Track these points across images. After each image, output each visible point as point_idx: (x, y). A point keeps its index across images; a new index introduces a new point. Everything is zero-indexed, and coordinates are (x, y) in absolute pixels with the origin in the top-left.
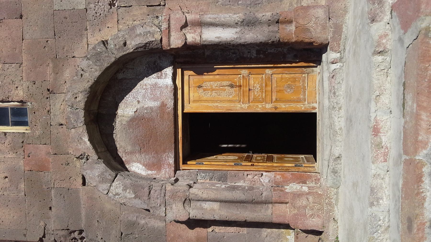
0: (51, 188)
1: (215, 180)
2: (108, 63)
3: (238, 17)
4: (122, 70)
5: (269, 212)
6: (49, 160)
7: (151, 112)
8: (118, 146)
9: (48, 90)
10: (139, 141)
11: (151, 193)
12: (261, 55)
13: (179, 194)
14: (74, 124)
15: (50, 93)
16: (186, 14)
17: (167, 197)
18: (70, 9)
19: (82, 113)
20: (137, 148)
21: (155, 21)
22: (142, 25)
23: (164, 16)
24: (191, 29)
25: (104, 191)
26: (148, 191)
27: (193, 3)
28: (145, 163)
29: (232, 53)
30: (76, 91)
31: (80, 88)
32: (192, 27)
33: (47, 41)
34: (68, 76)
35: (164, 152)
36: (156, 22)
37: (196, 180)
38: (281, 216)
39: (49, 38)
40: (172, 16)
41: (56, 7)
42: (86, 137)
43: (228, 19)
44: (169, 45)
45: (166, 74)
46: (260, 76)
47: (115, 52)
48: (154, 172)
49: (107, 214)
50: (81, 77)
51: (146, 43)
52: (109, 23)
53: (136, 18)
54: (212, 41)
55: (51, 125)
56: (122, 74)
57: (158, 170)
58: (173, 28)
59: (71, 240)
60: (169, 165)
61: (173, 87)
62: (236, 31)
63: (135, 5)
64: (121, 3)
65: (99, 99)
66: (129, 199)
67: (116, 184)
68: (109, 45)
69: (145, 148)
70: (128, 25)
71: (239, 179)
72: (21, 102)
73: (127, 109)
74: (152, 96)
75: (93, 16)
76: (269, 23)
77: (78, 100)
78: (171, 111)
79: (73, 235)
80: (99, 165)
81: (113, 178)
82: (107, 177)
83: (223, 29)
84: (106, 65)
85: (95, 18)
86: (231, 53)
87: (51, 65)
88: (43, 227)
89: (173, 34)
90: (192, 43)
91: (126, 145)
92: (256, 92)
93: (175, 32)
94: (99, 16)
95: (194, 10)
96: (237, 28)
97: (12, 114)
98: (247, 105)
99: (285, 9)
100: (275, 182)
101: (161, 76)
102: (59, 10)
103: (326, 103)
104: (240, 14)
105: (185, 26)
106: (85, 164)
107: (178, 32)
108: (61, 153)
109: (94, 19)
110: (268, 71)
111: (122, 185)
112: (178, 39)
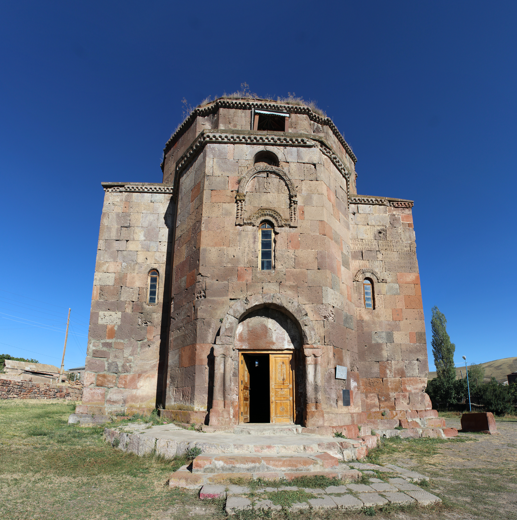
3: (319, 383)
5: (219, 399)
8: (251, 319)
9: (281, 282)
13: (228, 352)
17: (226, 345)
20: (251, 329)
35: (249, 344)
36: (317, 341)
40: (320, 350)
44: (305, 348)
46: (289, 394)
47: (302, 320)
60: (242, 346)
71: (235, 383)
72: (274, 267)
76: (316, 398)
79: (202, 292)
84: (295, 315)
87: (294, 284)
88: (207, 275)
89: (311, 350)
92: (280, 392)
97: (267, 261)
98: (273, 387)
103: (276, 427)
105: (315, 356)
110: (291, 398)
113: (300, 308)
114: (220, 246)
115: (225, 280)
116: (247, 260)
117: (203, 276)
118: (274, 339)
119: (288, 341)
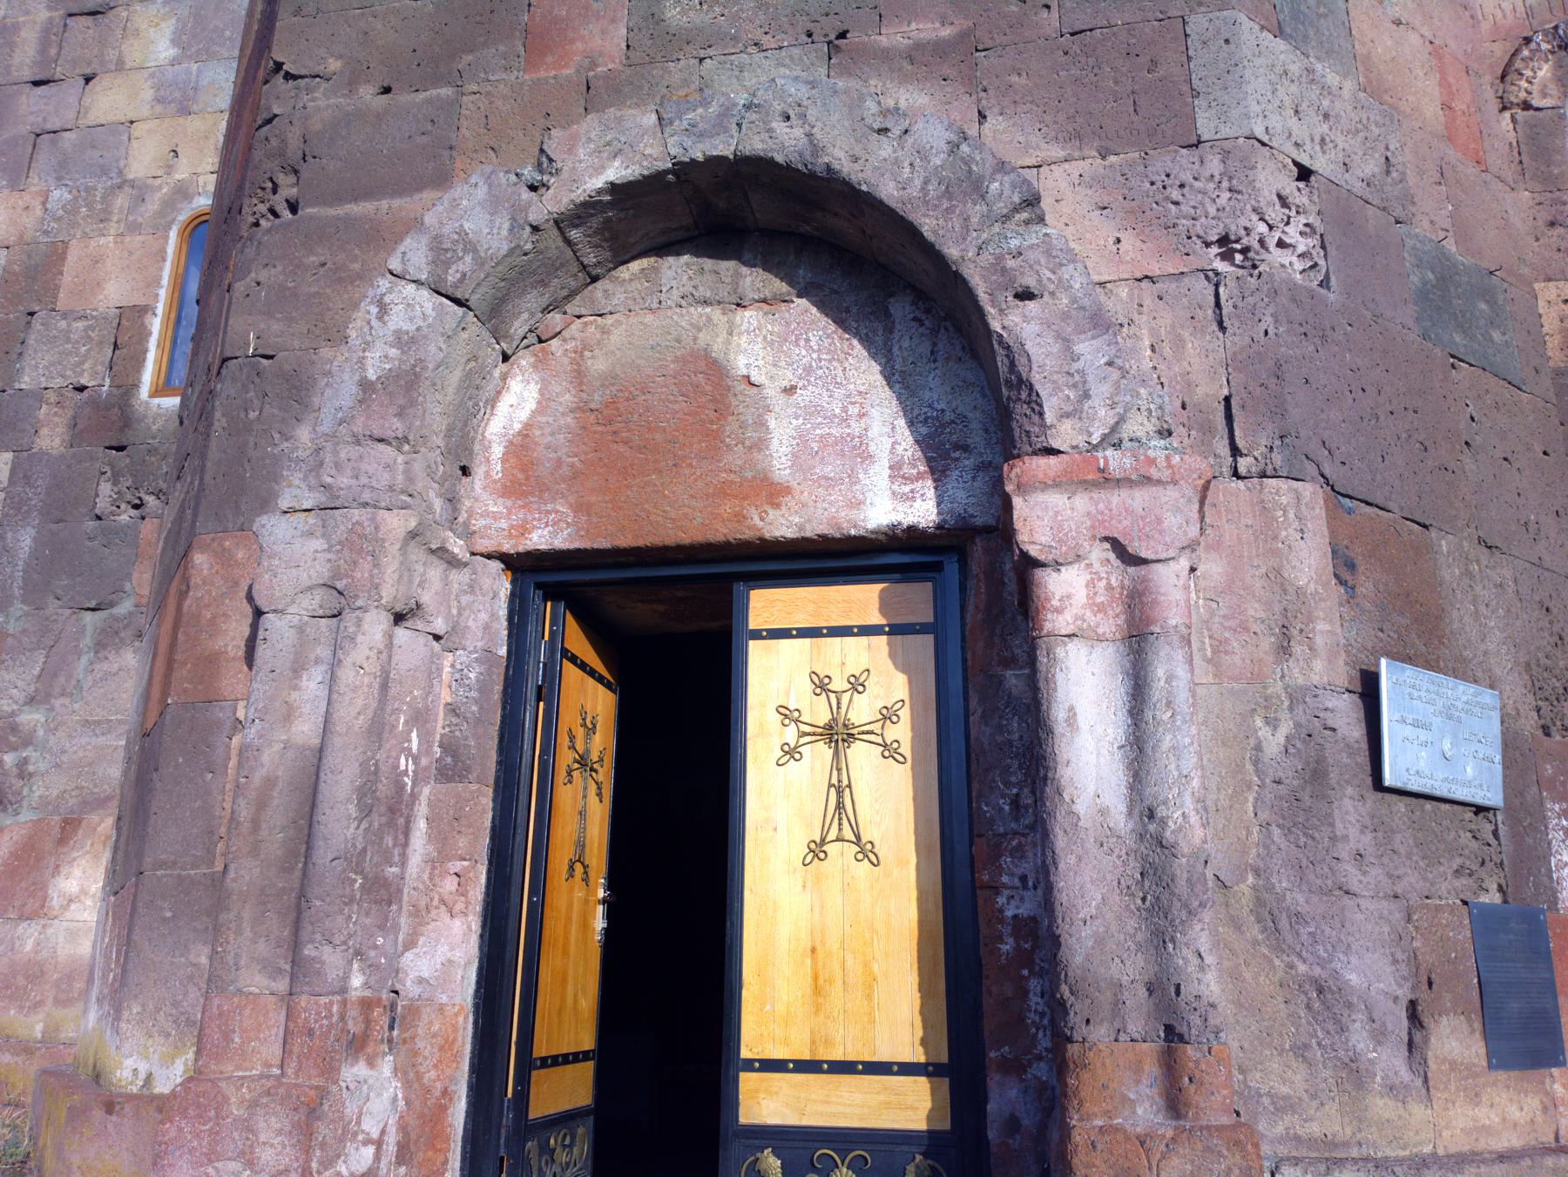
0: (459, 83)
1: (447, 729)
2: (935, 232)
4: (928, 311)
6: (566, 66)
7: (747, 443)
9: (842, 35)
10: (628, 400)
11: (381, 446)
12: (1011, 941)
14: (677, 123)
15: (829, 43)
16: (1184, 563)
18: (1193, 77)
19: (721, 147)
20: (597, 399)
21: (1146, 422)
22: (1116, 360)
23: (1168, 458)
24: (1109, 587)
25: (399, 260)
26: (389, 434)
27: (1256, 605)
28: (537, 433)
29: (1017, 795)
30: (812, 114)
31: (828, 129)
32: (1121, 594)
33: (1048, 7)
35: (580, 508)
36: (1139, 426)
37: (450, 645)
38: (227, 1037)
39: (1062, 11)
40: (1171, 494)
41: (1198, 23)
42: (623, 173)
43: (1172, 767)
45: (913, 499)
48: (499, 468)
49: (346, 296)
50: (876, 127)
51: (1031, 387)
52: (1138, 243)
53: (1167, 351)
54: (1055, 690)
55: (701, 60)
56: (911, 316)
58: (1109, 502)
59: (268, 175)
60: (523, 530)
61: (853, 532)
62: (1113, 810)
63: (1228, 344)
64: (1231, 283)
65: (801, 230)
66: (361, 361)
67: (426, 304)
68: (1021, 230)
69: (600, 428)
70: (1131, 322)
73: (760, 346)
74: (815, 446)
75: (1168, 176)
77: (774, 125)
79: (284, 180)
80: (505, 233)
82: (454, 267)
84: (928, 225)
85: (1160, 185)
86: (1015, 791)
87: (946, 32)
88: (319, 69)
90: (1038, 597)
91: (613, 352)
94: (1167, 198)
95: (1222, 613)
96: (1130, 814)
99: (1258, 1075)
100: (413, 1011)
101: (903, 477)
104: (1199, 833)
105: (1127, 557)
106: (513, 178)
107: (1092, 527)
108: (589, 107)
111: (418, 329)
112: (1057, 527)
113: (967, 162)
115: (437, 81)
117: (295, 77)
118: (779, 458)
119: (895, 467)
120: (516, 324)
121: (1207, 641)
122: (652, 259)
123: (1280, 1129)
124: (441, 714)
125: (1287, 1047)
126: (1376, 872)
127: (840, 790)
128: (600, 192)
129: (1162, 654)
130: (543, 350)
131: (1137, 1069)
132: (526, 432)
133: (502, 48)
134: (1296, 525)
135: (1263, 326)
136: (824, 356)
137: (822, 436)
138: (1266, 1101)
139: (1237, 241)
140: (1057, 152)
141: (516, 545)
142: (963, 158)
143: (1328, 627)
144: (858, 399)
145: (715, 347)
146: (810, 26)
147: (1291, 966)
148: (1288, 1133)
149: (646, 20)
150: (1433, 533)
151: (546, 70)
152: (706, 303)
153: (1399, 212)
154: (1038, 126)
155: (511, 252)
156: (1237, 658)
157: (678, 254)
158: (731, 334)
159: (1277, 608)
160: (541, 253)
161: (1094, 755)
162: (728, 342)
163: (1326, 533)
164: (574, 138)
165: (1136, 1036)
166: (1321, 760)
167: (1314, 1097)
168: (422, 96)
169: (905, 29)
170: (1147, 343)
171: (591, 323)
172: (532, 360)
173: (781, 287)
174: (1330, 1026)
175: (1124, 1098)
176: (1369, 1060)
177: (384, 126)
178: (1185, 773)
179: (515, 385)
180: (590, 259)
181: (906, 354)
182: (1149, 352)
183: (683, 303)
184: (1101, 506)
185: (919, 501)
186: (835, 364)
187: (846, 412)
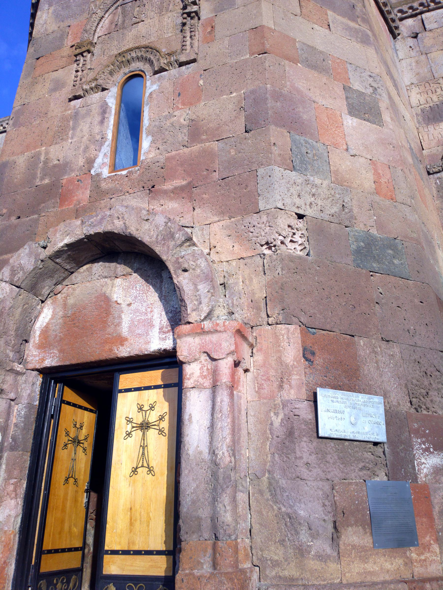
6: (71, 205)
7: (115, 324)
9: (153, 187)
14: (87, 223)
15: (149, 190)
21: (223, 310)
24: (208, 369)
27: (273, 371)
30: (126, 216)
32: (211, 371)
33: (215, 171)
34: (170, 207)
35: (61, 351)
37: (17, 402)
40: (224, 335)
41: (261, 171)
48: (38, 339)
52: (240, 247)
55: (111, 199)
56: (168, 277)
57: (39, 345)
58: (206, 339)
60: (43, 360)
61: (146, 353)
62: (204, 452)
68: (186, 249)
69: (70, 323)
74: (136, 323)
77: (115, 221)
78: (113, 354)
81: (14, 283)
82: (17, 276)
83: (208, 428)
84: (158, 249)
85: (247, 227)
87: (184, 183)
93: (199, 344)
94: (249, 231)
95: (261, 374)
99: (267, 552)
101: (163, 332)
102: (257, 176)
106: (37, 245)
107: (200, 348)
109: (245, 225)
111: (4, 297)
114: (35, 148)
115: (33, 213)
116: (84, 160)
120: (44, 291)
121: (256, 385)
122: (90, 265)
123: (274, 573)
124: (13, 427)
125: (277, 541)
126: (315, 471)
127: (144, 447)
128: (62, 247)
129: (220, 393)
130: (55, 298)
131: (205, 551)
132: (46, 327)
133: (53, 201)
134: (287, 341)
135: (278, 272)
136: (141, 292)
137: (139, 320)
138: (269, 562)
139: (272, 243)
140: (216, 219)
141: (40, 366)
142: (169, 227)
143: (298, 377)
144: (150, 306)
145: (107, 292)
146: (144, 185)
147: (280, 509)
148: (276, 575)
149: (95, 187)
150: (356, 338)
151: (65, 207)
152: (106, 277)
153: (347, 223)
154: (211, 210)
155: (34, 269)
156: (265, 392)
157: (98, 262)
158: (112, 287)
159: (279, 371)
160: (47, 268)
161: (198, 432)
162: (111, 290)
163: (300, 342)
164: (56, 231)
165: (206, 538)
166: (292, 428)
167: (286, 560)
168: (28, 218)
169: (172, 183)
170: (241, 280)
171: (70, 287)
172: (51, 301)
173: (129, 270)
174: (293, 532)
175: (199, 562)
176: (308, 546)
177: (17, 229)
178: (224, 436)
179: (45, 310)
180: (68, 267)
181: (166, 289)
182: (241, 283)
183: (99, 278)
184: (203, 341)
185: (167, 340)
186: (144, 294)
187: (146, 311)
